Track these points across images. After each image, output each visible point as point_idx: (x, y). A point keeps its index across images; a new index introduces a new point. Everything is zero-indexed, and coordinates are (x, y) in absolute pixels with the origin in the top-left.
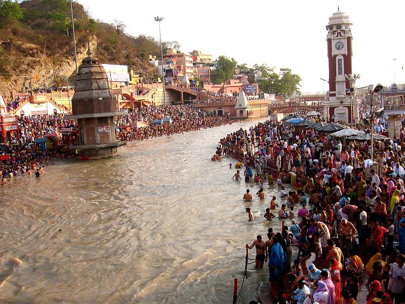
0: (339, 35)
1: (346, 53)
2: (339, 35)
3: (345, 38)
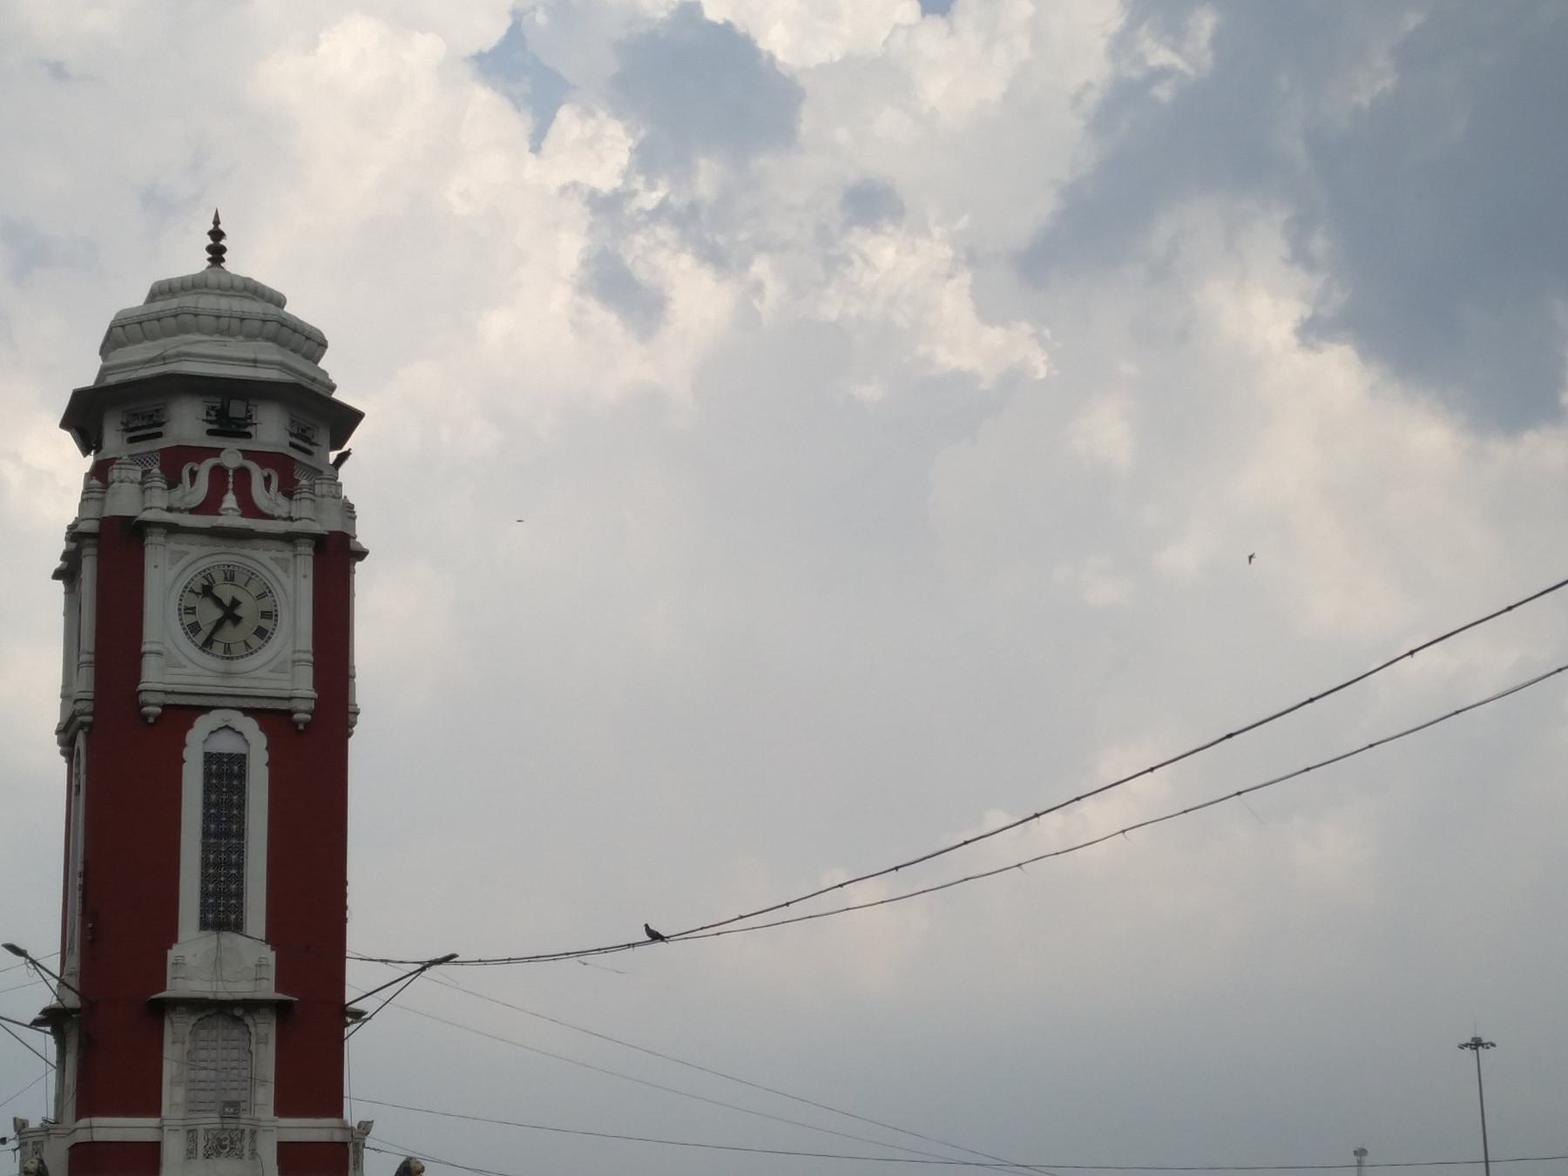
0: (230, 501)
1: (300, 685)
2: (230, 501)
3: (290, 538)
